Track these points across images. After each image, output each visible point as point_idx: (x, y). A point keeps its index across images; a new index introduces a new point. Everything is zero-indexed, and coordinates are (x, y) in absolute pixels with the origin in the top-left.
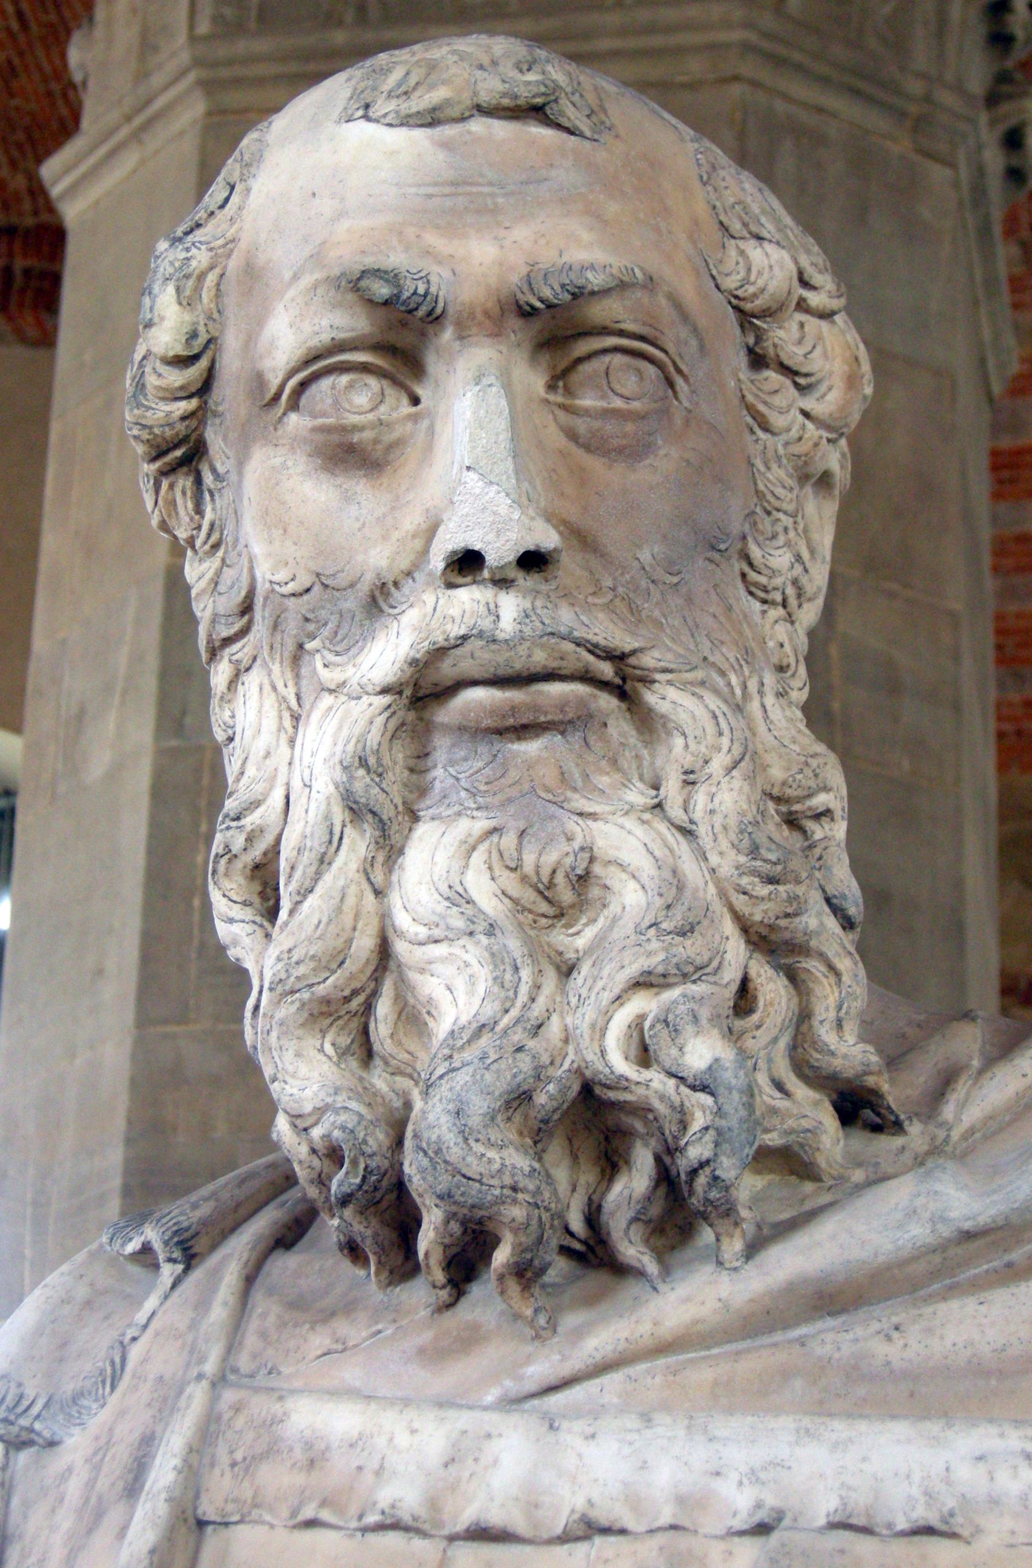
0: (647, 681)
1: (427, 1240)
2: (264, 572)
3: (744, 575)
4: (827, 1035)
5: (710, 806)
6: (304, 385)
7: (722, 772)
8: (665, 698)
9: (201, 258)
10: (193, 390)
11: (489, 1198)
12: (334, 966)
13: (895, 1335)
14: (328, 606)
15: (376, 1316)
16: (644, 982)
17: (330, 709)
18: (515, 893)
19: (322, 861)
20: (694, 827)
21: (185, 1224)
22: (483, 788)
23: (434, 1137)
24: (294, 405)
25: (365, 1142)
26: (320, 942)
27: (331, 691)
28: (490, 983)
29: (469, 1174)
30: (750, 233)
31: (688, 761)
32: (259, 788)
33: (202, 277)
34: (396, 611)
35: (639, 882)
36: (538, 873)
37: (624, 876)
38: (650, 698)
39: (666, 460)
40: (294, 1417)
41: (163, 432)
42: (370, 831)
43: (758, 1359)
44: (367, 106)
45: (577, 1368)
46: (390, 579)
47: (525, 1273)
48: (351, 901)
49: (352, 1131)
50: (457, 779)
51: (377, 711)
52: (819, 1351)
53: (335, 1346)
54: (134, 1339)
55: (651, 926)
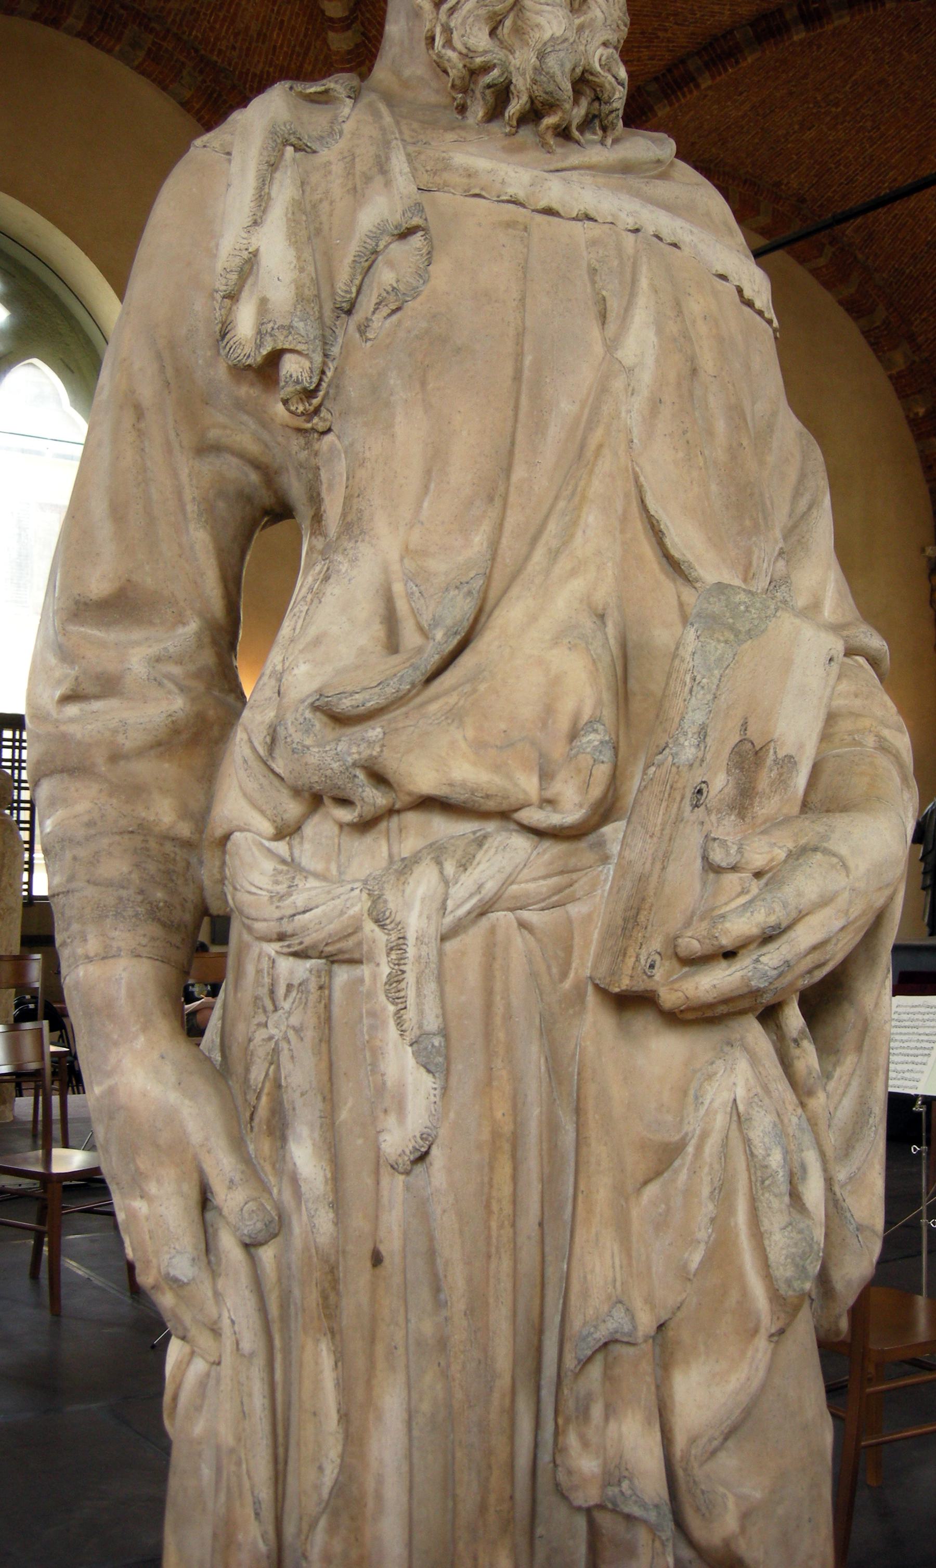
1: (514, 108)
40: (456, 159)
43: (616, 179)
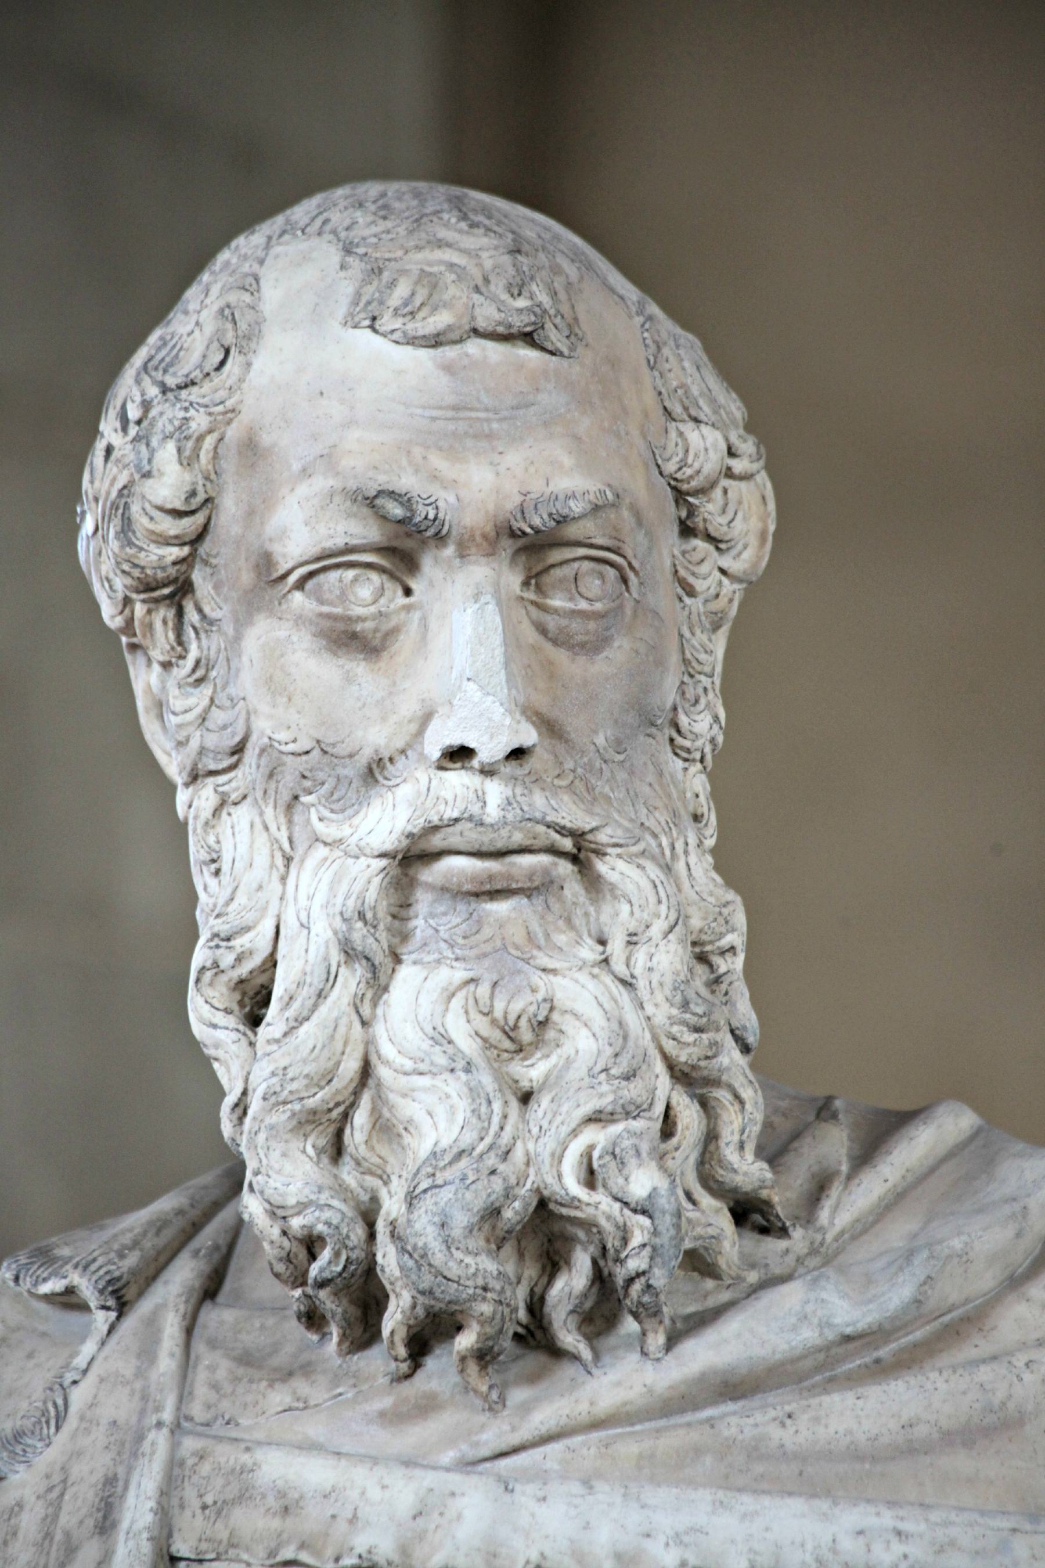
0: (600, 853)
2: (263, 727)
3: (672, 740)
4: (731, 1155)
5: (649, 964)
6: (311, 575)
7: (660, 936)
8: (611, 868)
9: (199, 421)
10: (187, 540)
11: (464, 1296)
12: (323, 1083)
13: (788, 1422)
14: (327, 769)
15: (336, 1380)
16: (596, 1118)
17: (326, 859)
18: (485, 1033)
19: (319, 996)
20: (634, 981)
21: (117, 1274)
22: (461, 941)
23: (420, 1244)
24: (300, 585)
25: (348, 1237)
26: (314, 1064)
27: (325, 844)
28: (469, 1114)
29: (449, 1276)
30: (690, 416)
31: (632, 927)
32: (249, 917)
33: (200, 439)
34: (390, 783)
35: (590, 1030)
36: (505, 1018)
37: (577, 1023)
38: (602, 867)
39: (620, 650)
40: (265, 1468)
41: (155, 574)
42: (360, 970)
43: (675, 1436)
44: (374, 319)
45: (525, 1438)
46: (386, 755)
47: (484, 1356)
48: (342, 1029)
49: (337, 1228)
50: (437, 931)
51: (375, 873)
52: (726, 1433)
53: (296, 1404)
54: (75, 1382)
55: (602, 1071)
